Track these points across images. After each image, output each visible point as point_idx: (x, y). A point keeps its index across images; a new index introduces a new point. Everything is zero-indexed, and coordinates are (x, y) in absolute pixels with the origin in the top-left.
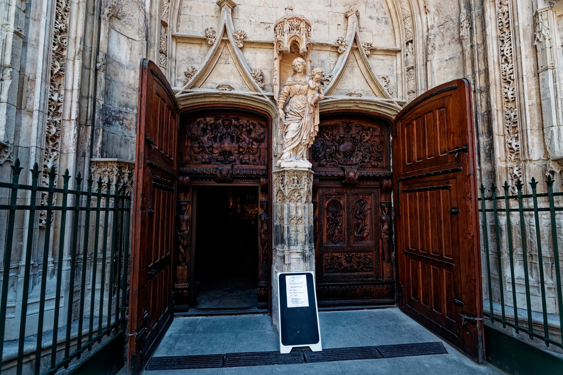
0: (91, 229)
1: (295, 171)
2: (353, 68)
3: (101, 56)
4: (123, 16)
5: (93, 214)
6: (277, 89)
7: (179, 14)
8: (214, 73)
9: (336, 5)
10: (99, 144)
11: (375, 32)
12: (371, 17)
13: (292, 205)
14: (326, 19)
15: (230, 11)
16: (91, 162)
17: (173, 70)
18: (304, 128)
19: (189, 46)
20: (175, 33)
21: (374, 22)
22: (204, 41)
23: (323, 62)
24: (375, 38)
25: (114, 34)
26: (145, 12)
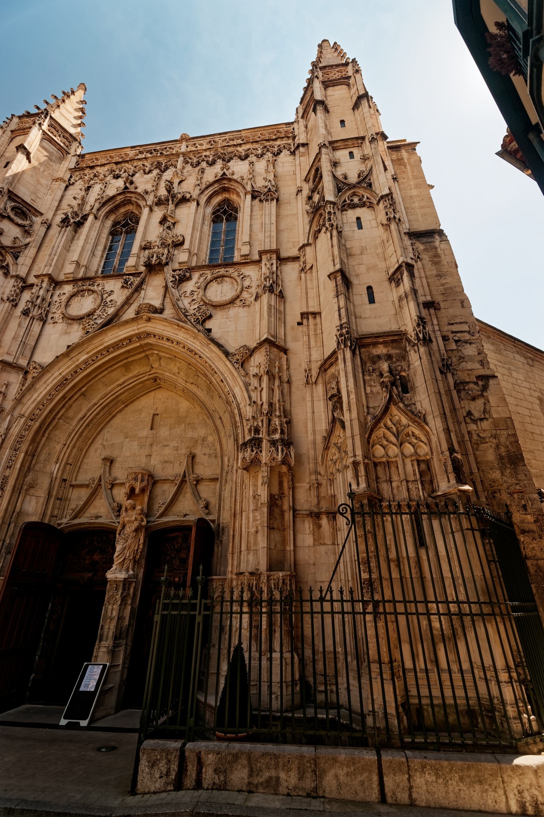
1: (115, 581)
2: (186, 493)
3: (15, 514)
4: (37, 485)
7: (80, 468)
8: (92, 506)
9: (181, 448)
11: (206, 465)
12: (205, 454)
13: (110, 607)
14: (173, 459)
15: (109, 464)
17: (66, 507)
18: (127, 548)
20: (74, 483)
21: (207, 457)
22: (87, 486)
23: (164, 491)
25: (28, 498)
26: (52, 478)
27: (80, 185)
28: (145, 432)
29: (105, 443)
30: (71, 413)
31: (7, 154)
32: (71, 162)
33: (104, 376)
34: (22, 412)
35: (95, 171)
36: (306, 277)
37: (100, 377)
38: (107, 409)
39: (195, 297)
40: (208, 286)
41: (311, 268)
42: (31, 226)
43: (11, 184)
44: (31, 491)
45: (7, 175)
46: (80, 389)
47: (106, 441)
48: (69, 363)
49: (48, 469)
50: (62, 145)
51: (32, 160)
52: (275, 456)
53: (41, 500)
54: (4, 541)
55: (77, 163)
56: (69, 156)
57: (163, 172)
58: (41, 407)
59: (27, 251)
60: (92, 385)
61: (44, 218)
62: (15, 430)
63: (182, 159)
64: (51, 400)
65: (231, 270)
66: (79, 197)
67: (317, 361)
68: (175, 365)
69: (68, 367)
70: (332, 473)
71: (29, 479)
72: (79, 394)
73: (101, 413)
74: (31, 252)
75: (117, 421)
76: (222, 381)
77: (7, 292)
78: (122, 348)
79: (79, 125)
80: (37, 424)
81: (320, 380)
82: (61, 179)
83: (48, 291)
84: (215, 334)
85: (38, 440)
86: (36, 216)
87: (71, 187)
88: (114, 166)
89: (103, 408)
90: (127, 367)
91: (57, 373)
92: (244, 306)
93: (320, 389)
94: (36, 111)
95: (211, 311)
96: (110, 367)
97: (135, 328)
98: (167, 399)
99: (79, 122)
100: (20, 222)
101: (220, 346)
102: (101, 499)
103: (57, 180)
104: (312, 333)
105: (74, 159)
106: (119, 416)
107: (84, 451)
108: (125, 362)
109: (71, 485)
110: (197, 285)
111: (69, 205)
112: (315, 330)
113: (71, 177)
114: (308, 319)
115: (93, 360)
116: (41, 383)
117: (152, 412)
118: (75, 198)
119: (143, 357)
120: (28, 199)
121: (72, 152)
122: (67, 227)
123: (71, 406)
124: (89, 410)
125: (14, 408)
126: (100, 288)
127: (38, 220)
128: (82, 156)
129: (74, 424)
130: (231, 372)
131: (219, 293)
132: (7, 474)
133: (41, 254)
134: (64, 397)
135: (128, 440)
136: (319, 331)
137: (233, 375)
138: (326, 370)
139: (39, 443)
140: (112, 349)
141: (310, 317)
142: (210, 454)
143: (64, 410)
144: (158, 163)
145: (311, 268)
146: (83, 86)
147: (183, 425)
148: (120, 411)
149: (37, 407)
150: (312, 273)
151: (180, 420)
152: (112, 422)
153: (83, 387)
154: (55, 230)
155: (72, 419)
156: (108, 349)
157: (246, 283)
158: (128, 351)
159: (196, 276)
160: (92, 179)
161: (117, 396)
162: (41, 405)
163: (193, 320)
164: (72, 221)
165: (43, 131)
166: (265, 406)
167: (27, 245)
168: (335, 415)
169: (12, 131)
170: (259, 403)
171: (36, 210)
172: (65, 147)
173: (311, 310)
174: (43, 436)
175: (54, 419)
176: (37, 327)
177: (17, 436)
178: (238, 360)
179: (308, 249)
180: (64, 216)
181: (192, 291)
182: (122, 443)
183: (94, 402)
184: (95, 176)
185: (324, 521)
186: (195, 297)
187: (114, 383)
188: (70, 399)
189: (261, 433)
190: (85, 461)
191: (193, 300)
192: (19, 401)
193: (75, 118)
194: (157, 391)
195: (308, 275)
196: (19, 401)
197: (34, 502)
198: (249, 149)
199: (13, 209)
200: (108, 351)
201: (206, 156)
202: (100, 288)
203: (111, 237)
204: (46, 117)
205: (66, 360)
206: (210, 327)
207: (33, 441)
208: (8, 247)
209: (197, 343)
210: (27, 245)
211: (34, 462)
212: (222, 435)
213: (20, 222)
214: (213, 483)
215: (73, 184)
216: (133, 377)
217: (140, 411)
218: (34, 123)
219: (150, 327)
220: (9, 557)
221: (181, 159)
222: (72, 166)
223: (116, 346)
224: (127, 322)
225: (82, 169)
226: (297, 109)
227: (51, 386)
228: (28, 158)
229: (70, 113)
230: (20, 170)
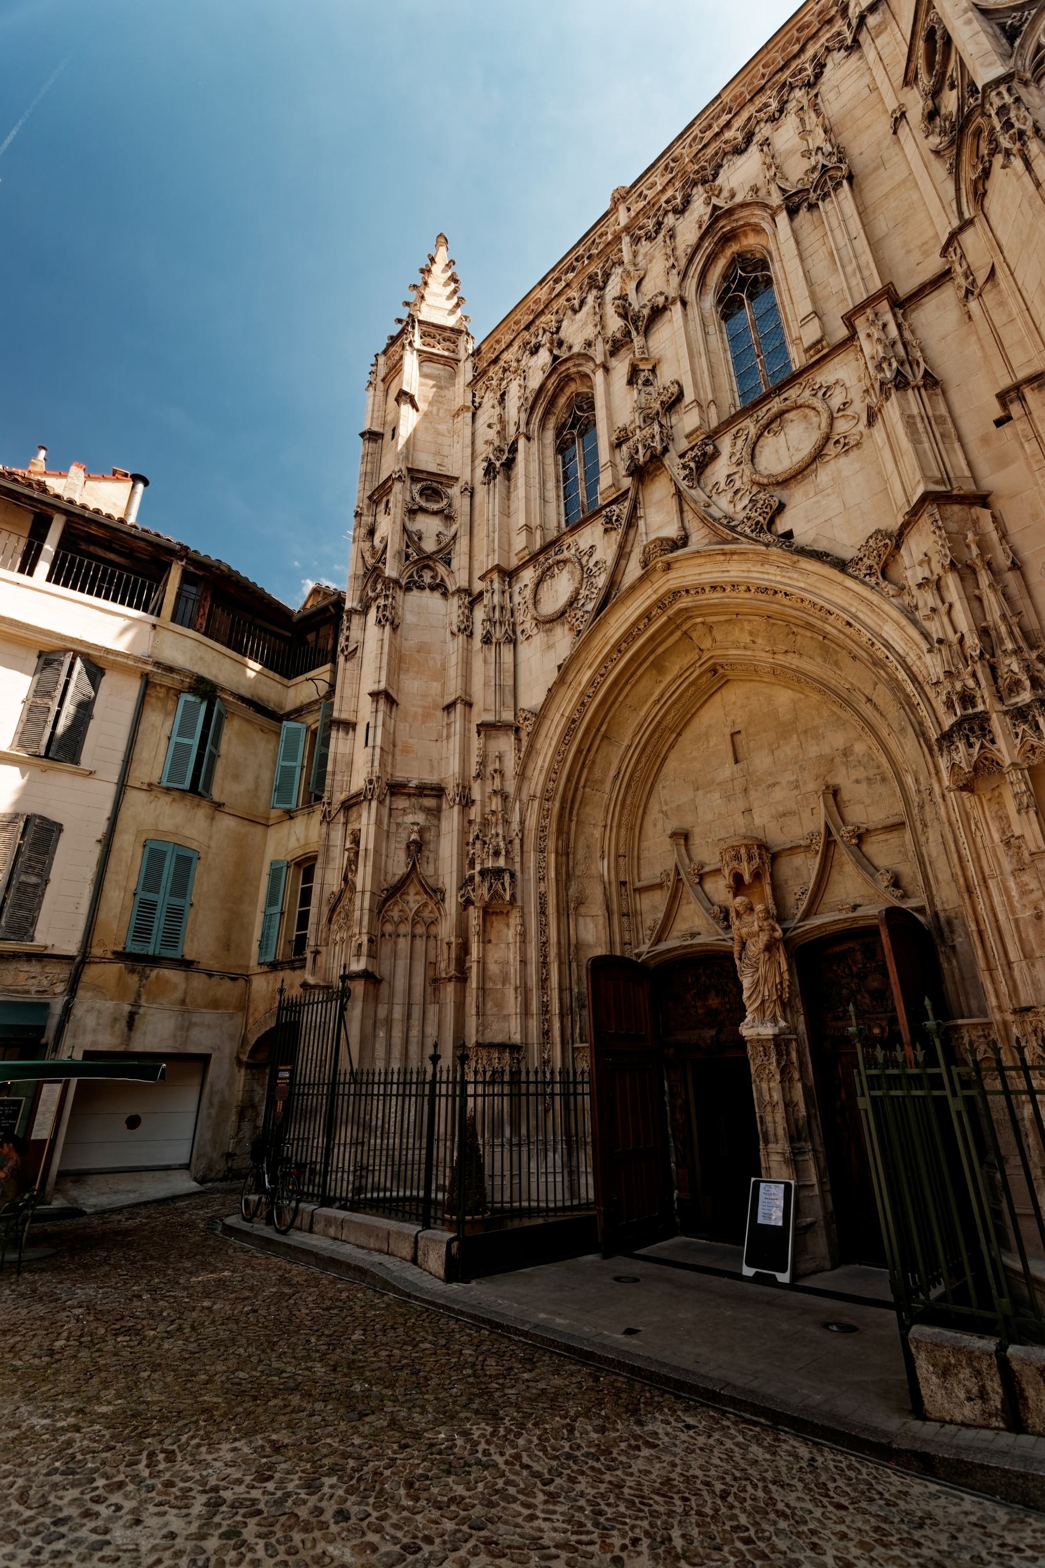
0: (579, 1112)
1: (758, 1041)
2: (842, 865)
3: (572, 948)
5: (579, 1098)
7: (639, 858)
8: (678, 919)
10: (578, 1031)
11: (868, 801)
12: (857, 781)
14: (794, 807)
15: (682, 842)
16: (574, 1049)
18: (761, 981)
19: (651, 893)
20: (638, 885)
21: (864, 786)
22: (660, 886)
23: (797, 869)
24: (870, 809)
25: (581, 920)
27: (489, 399)
28: (727, 770)
29: (665, 808)
30: (597, 773)
31: (389, 418)
32: (466, 371)
33: (627, 695)
34: (532, 792)
35: (502, 363)
37: (621, 699)
38: (649, 749)
39: (738, 484)
40: (758, 449)
41: (993, 271)
42: (450, 506)
43: (407, 458)
44: (583, 910)
45: (399, 447)
46: (598, 730)
47: (666, 804)
49: (594, 871)
50: (446, 353)
51: (419, 405)
52: (1035, 741)
53: (601, 921)
54: (571, 990)
55: (475, 368)
56: (461, 364)
58: (553, 776)
59: (457, 546)
60: (613, 717)
61: (461, 483)
62: (532, 822)
64: (564, 760)
65: (793, 393)
66: (495, 420)
68: (742, 629)
69: (570, 701)
71: (571, 892)
72: (599, 737)
73: (643, 760)
74: (462, 544)
75: (672, 764)
76: (849, 624)
77: (455, 620)
78: (639, 636)
79: (458, 305)
80: (557, 804)
82: (464, 408)
83: (503, 592)
84: (803, 536)
85: (565, 828)
86: (451, 486)
87: (479, 412)
88: (526, 335)
89: (644, 749)
90: (659, 667)
91: (558, 716)
92: (847, 449)
94: (400, 327)
95: (779, 494)
96: (632, 676)
97: (650, 591)
98: (748, 698)
99: (455, 300)
100: (435, 507)
101: (819, 556)
102: (689, 903)
103: (457, 414)
105: (469, 365)
106: (672, 756)
107: (637, 830)
108: (652, 658)
109: (635, 890)
110: (734, 459)
111: (486, 442)
113: (474, 395)
114: (1022, 398)
115: (602, 675)
116: (541, 739)
117: (728, 731)
118: (490, 426)
119: (680, 638)
120: (433, 468)
121: (462, 355)
122: (495, 478)
123: (593, 762)
124: (622, 760)
125: (519, 789)
126: (573, 551)
127: (455, 491)
128: (477, 352)
129: (607, 790)
130: (863, 599)
131: (783, 451)
132: (542, 889)
133: (476, 540)
134: (579, 751)
135: (701, 792)
137: (870, 604)
139: (568, 834)
140: (624, 645)
141: (1027, 392)
142: (869, 779)
143: (586, 771)
145: (993, 271)
146: (442, 239)
147: (795, 737)
148: (672, 747)
149: (548, 779)
150: (996, 285)
151: (786, 729)
152: (665, 770)
153: (601, 724)
154: (481, 491)
155: (602, 782)
156: (618, 648)
157: (836, 401)
158: (652, 638)
159: (725, 444)
160: (502, 379)
161: (660, 723)
162: (553, 772)
163: (748, 531)
164: (498, 464)
165: (418, 351)
166: (972, 641)
167: (454, 537)
169: (383, 380)
170: (954, 638)
171: (448, 477)
172: (451, 355)
174: (571, 820)
175: (576, 789)
176: (507, 652)
177: (537, 829)
178: (870, 567)
179: (968, 238)
180: (485, 464)
181: (729, 476)
182: (694, 800)
183: (625, 744)
184: (505, 370)
186: (738, 484)
187: (646, 702)
188: (589, 751)
189: (980, 701)
190: (644, 844)
191: (736, 492)
192: (522, 776)
193: (449, 298)
194: (723, 690)
195: (989, 298)
196: (522, 776)
197: (591, 926)
198: (749, 119)
199: (421, 493)
200: (619, 651)
201: (667, 202)
202: (573, 551)
203: (560, 457)
204: (413, 327)
205: (563, 690)
206: (787, 529)
207: (560, 831)
208: (434, 553)
209: (772, 570)
210: (454, 537)
211: (571, 864)
212: (884, 732)
213: (435, 507)
214: (895, 834)
215: (480, 404)
216: (674, 680)
217: (707, 735)
218: (403, 347)
219: (675, 579)
220: (585, 1012)
221: (626, 240)
222: (469, 377)
223: (629, 636)
224: (633, 588)
225: (485, 372)
227: (555, 739)
228: (415, 406)
229: (440, 295)
230: (410, 430)
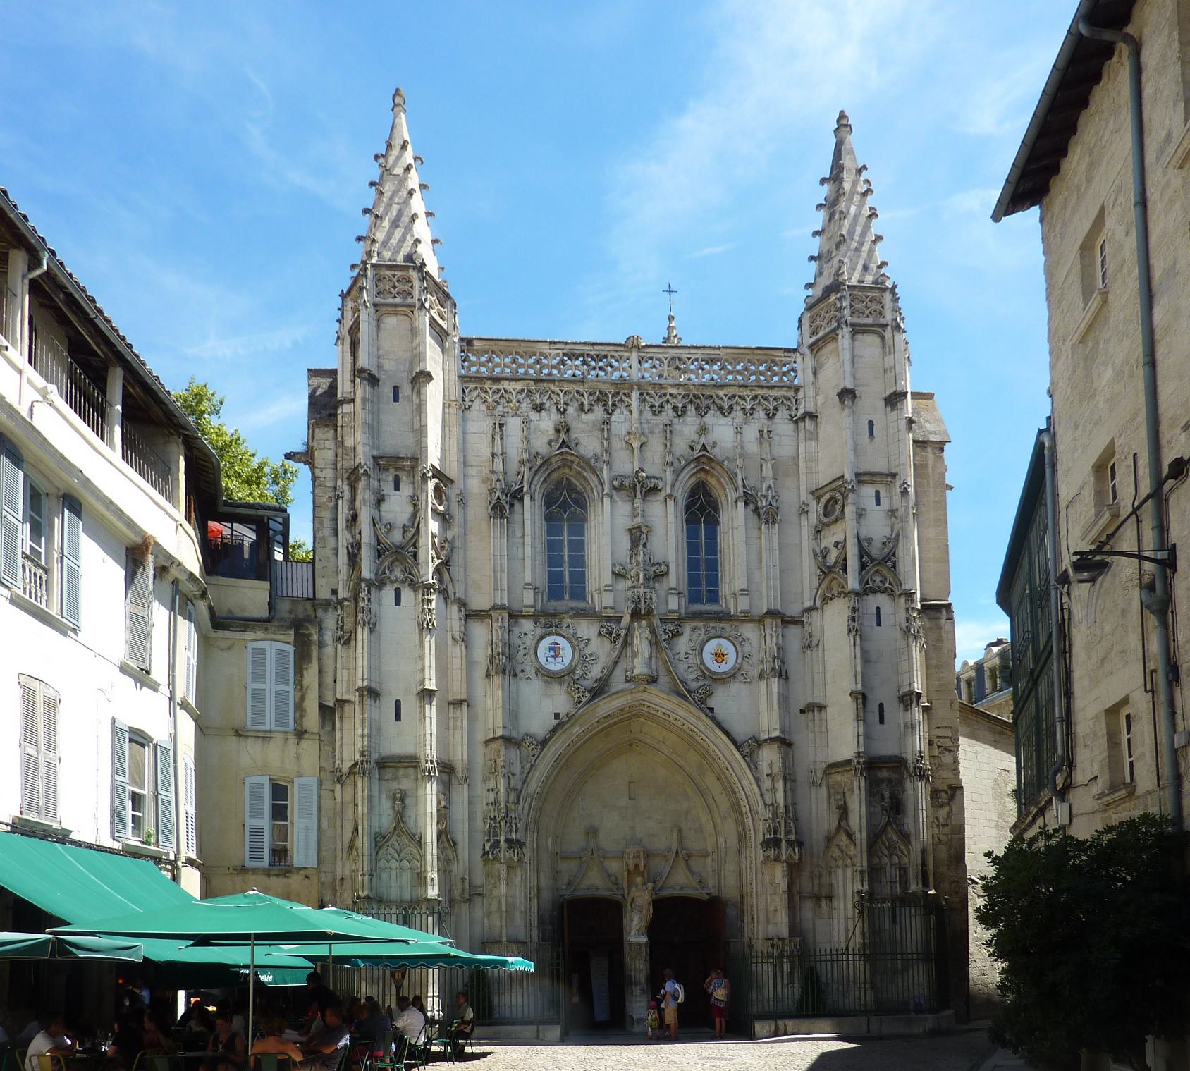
6: (626, 891)
36: (812, 654)
39: (690, 661)
48: (564, 737)
57: (610, 414)
63: (638, 393)
65: (726, 625)
67: (822, 762)
70: (831, 867)
81: (824, 782)
84: (719, 713)
93: (824, 791)
104: (817, 729)
112: (820, 727)
126: (571, 631)
136: (824, 729)
138: (830, 774)
141: (816, 710)
144: (600, 392)
145: (818, 644)
150: (818, 651)
157: (747, 650)
159: (687, 629)
163: (697, 699)
166: (782, 809)
168: (842, 824)
173: (816, 701)
179: (814, 613)
185: (823, 903)
186: (690, 661)
191: (689, 667)
195: (814, 653)
201: (671, 395)
202: (571, 631)
212: (717, 815)
221: (635, 394)
226: (800, 321)
